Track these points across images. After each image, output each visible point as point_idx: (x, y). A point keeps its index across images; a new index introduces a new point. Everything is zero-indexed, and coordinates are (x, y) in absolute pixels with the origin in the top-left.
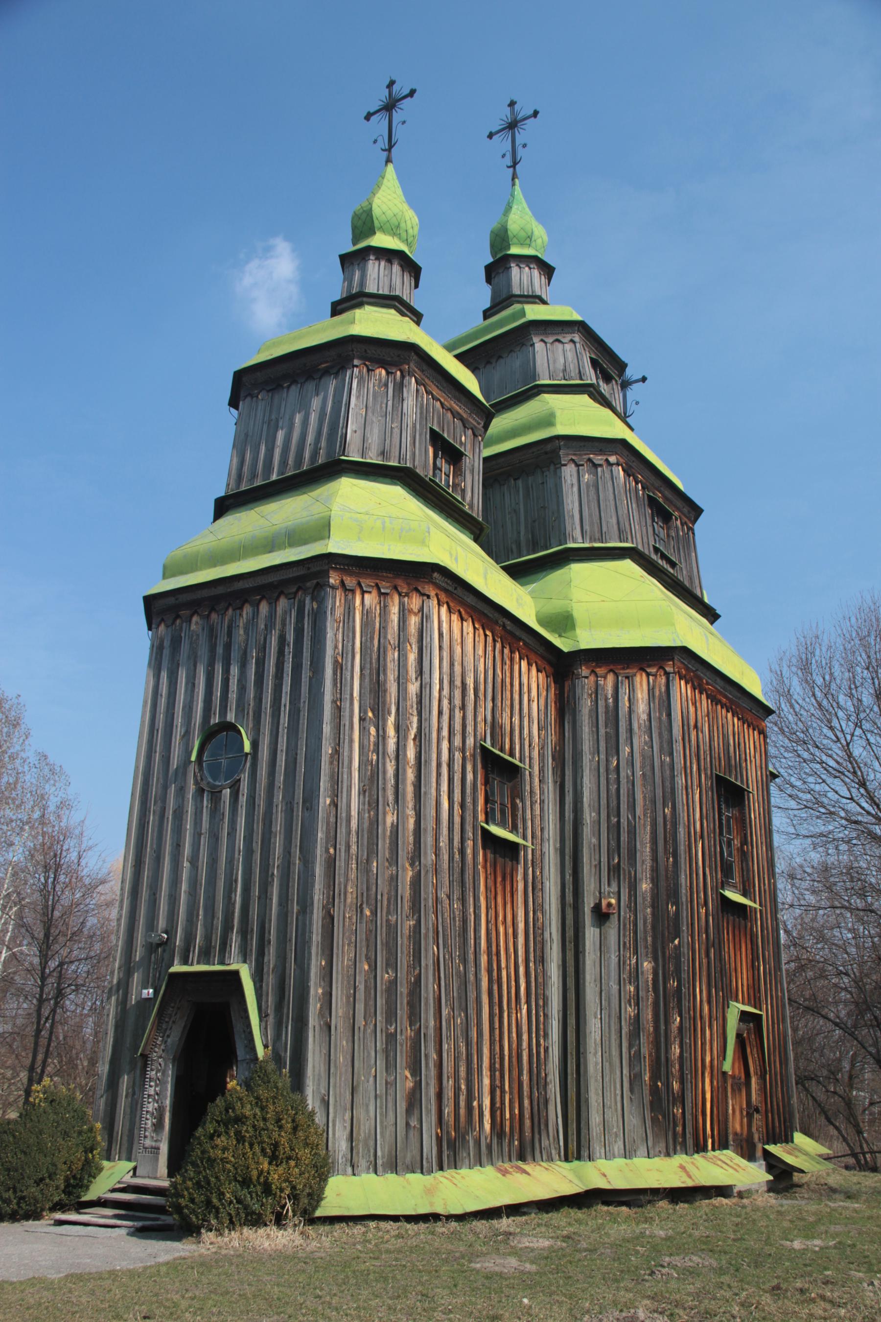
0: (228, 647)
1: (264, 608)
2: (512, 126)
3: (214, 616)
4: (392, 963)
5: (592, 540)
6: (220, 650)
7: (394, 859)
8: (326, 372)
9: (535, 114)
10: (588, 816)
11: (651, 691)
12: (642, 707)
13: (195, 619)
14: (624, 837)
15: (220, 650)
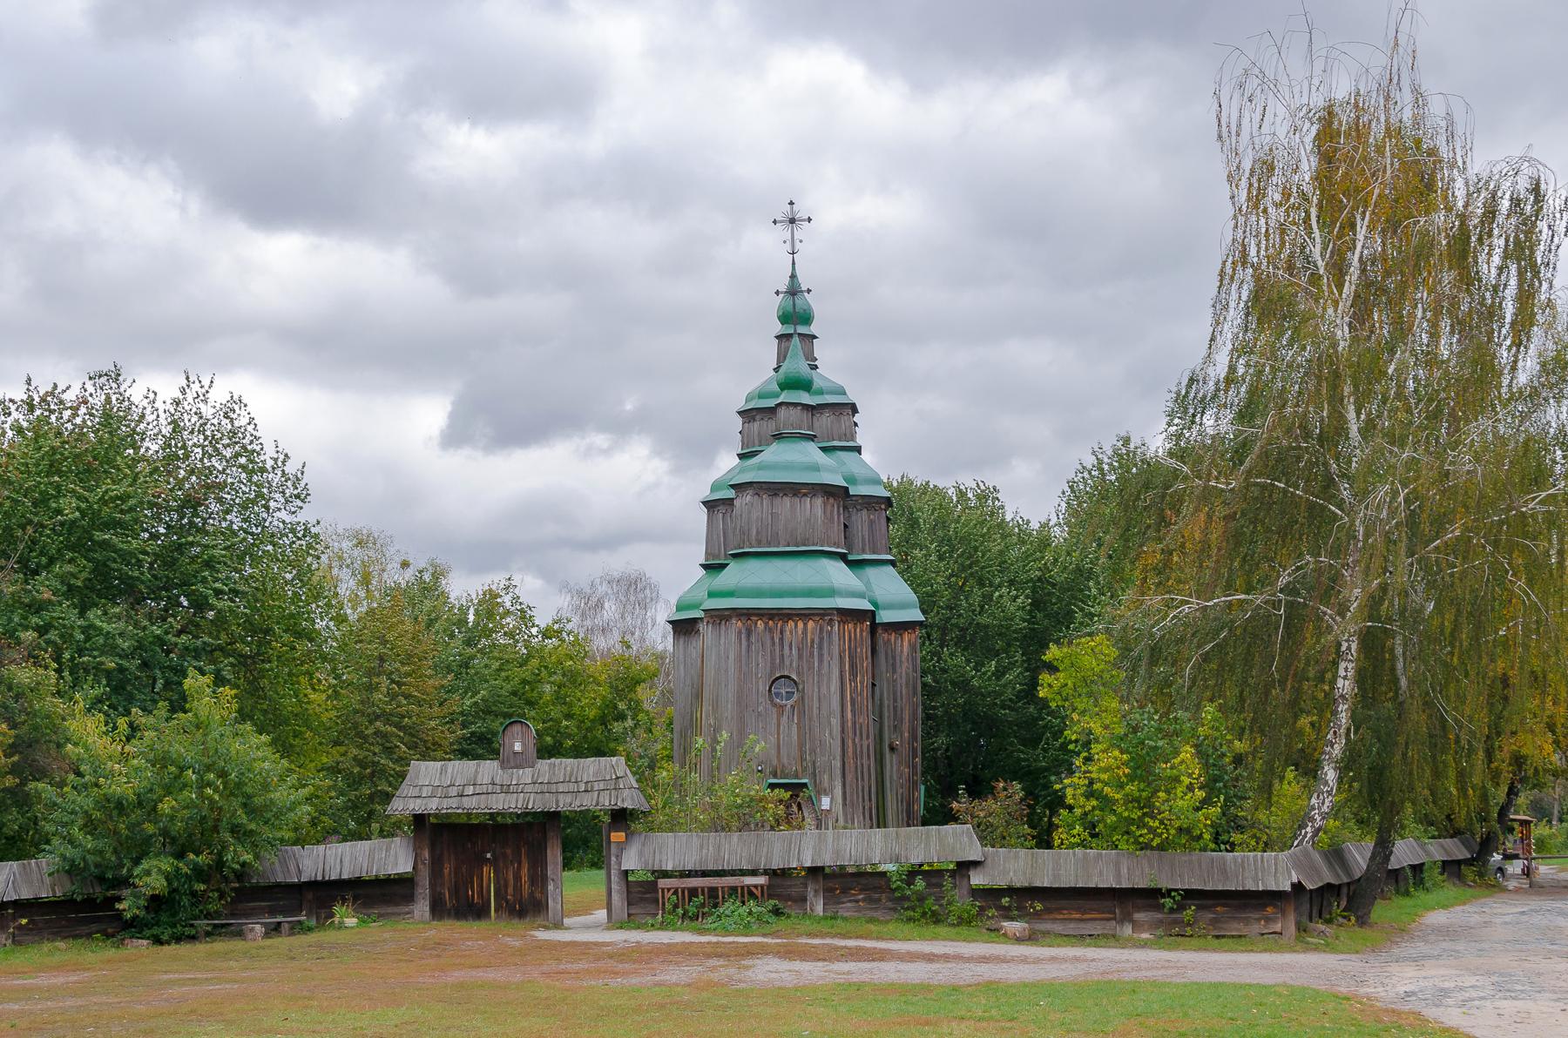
0: (781, 639)
1: (801, 625)
2: (792, 221)
3: (770, 622)
4: (863, 779)
5: (874, 553)
6: (777, 641)
7: (861, 739)
8: (805, 495)
9: (809, 220)
10: (886, 702)
11: (909, 641)
12: (905, 650)
13: (759, 622)
14: (899, 712)
15: (777, 641)
